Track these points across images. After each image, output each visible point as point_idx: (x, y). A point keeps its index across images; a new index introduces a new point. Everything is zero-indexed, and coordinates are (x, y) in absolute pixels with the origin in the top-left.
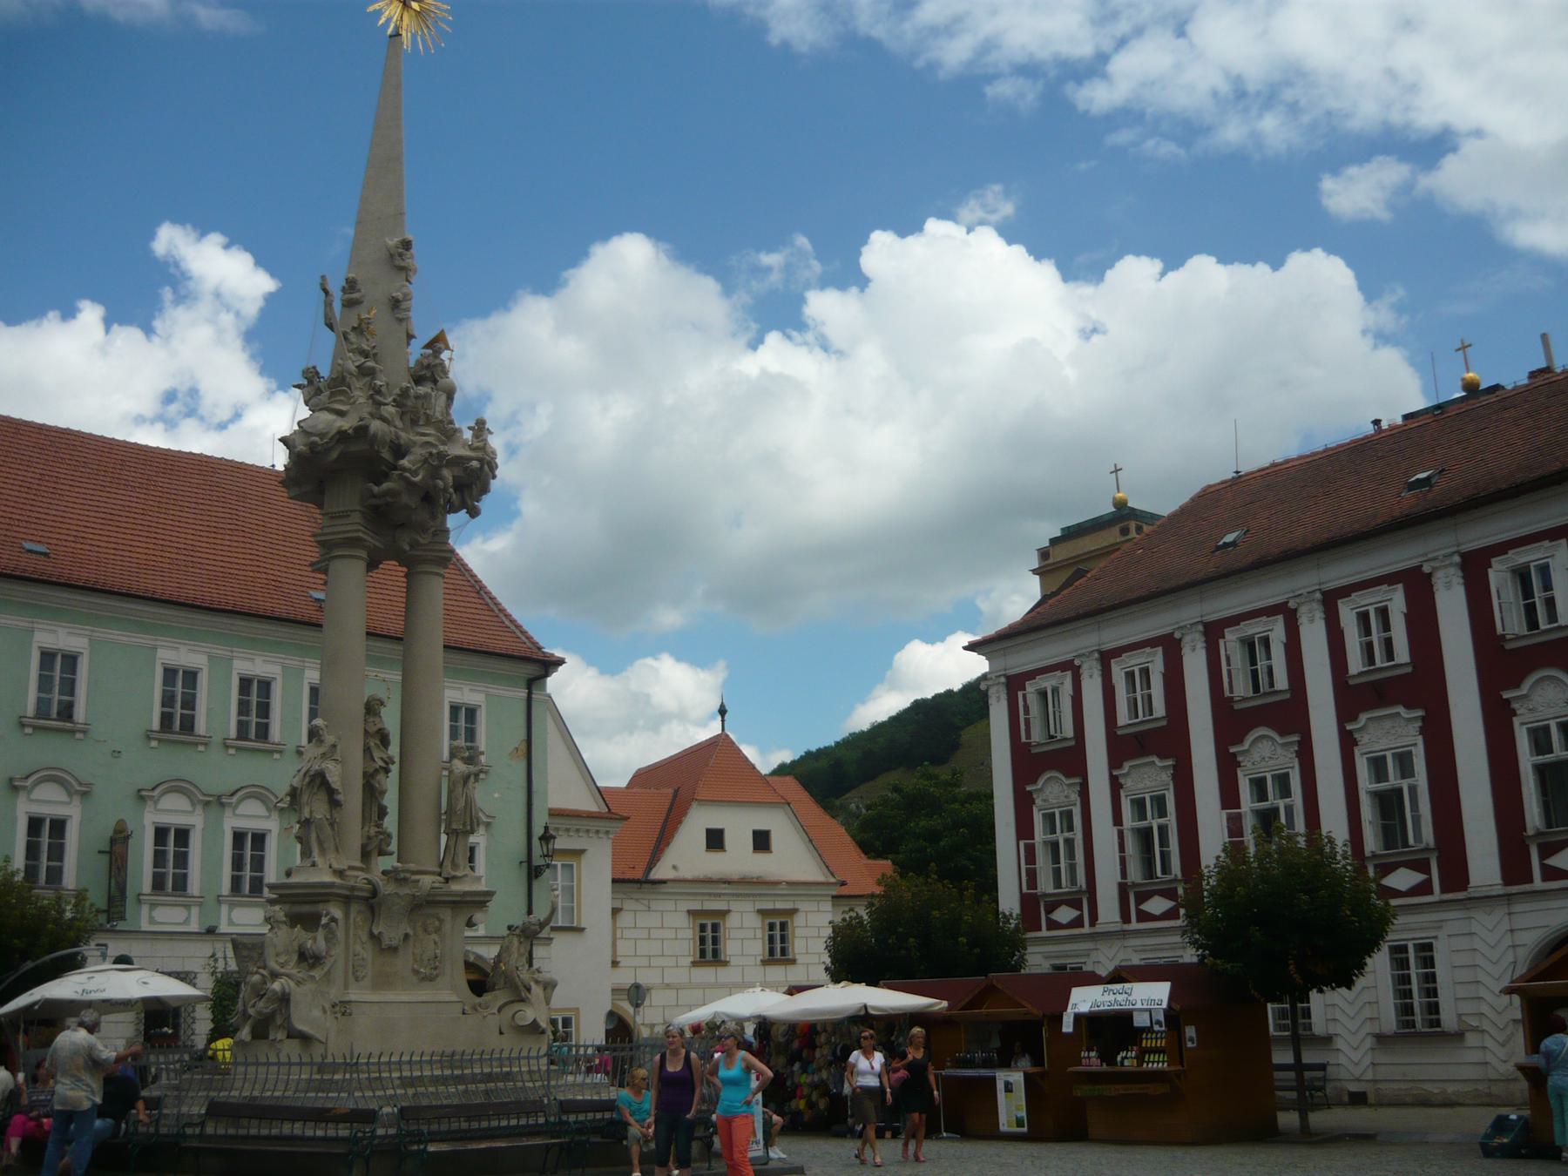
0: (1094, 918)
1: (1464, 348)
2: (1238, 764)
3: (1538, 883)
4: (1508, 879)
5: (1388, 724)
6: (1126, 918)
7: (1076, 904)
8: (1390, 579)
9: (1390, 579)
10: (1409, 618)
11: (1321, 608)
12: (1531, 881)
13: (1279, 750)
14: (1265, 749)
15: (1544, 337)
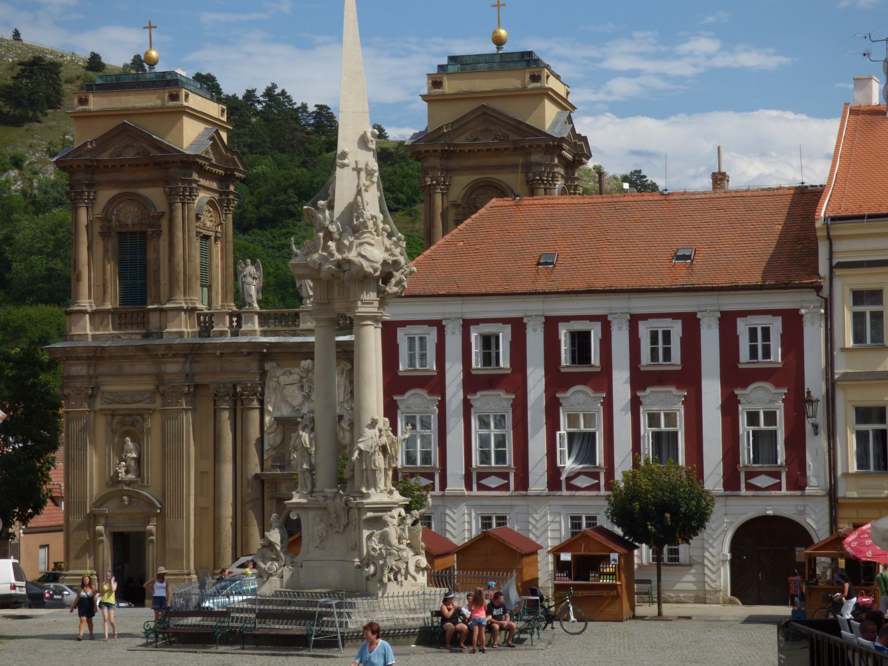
0: (443, 486)
1: (498, 6)
2: (561, 404)
3: (743, 491)
4: (727, 486)
5: (662, 395)
6: (469, 487)
7: (431, 476)
8: (674, 316)
9: (674, 316)
10: (683, 341)
11: (628, 324)
12: (739, 489)
13: (589, 400)
14: (581, 397)
15: (719, 148)
